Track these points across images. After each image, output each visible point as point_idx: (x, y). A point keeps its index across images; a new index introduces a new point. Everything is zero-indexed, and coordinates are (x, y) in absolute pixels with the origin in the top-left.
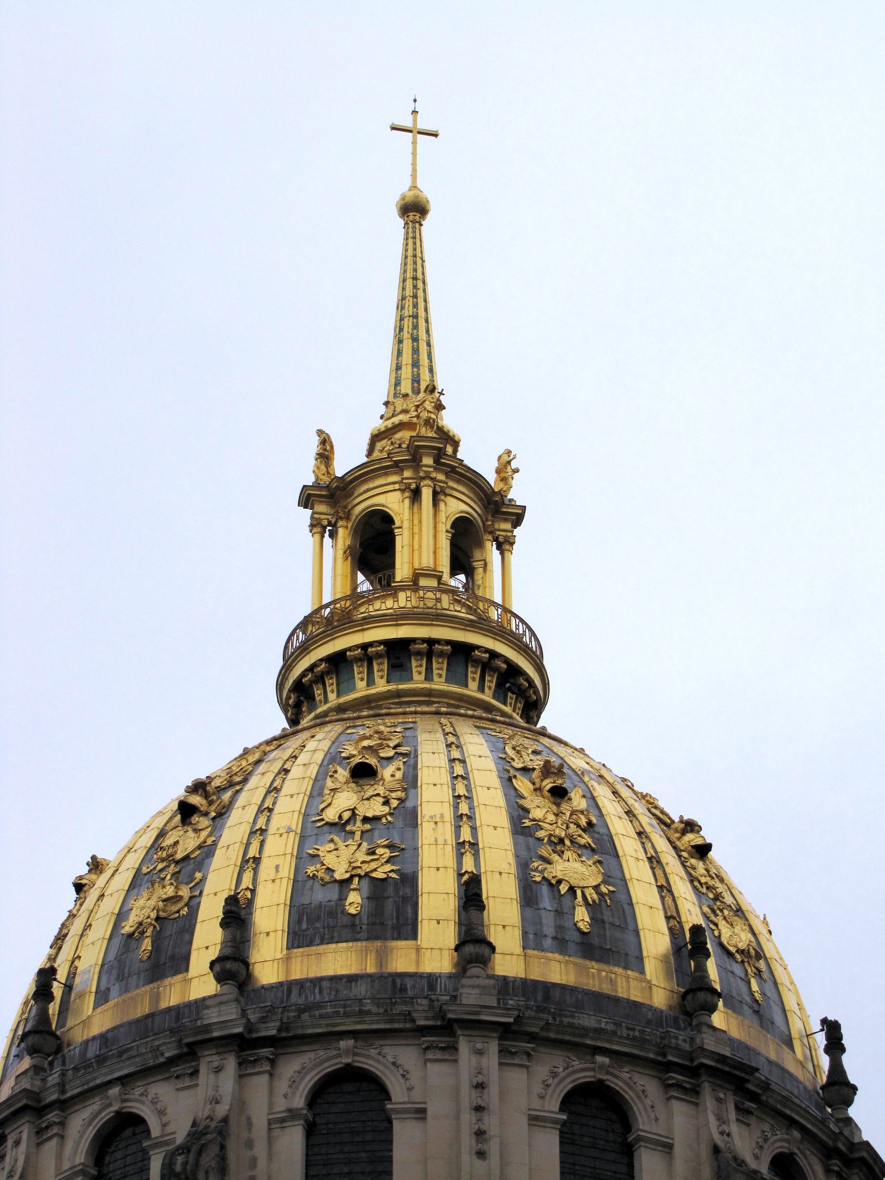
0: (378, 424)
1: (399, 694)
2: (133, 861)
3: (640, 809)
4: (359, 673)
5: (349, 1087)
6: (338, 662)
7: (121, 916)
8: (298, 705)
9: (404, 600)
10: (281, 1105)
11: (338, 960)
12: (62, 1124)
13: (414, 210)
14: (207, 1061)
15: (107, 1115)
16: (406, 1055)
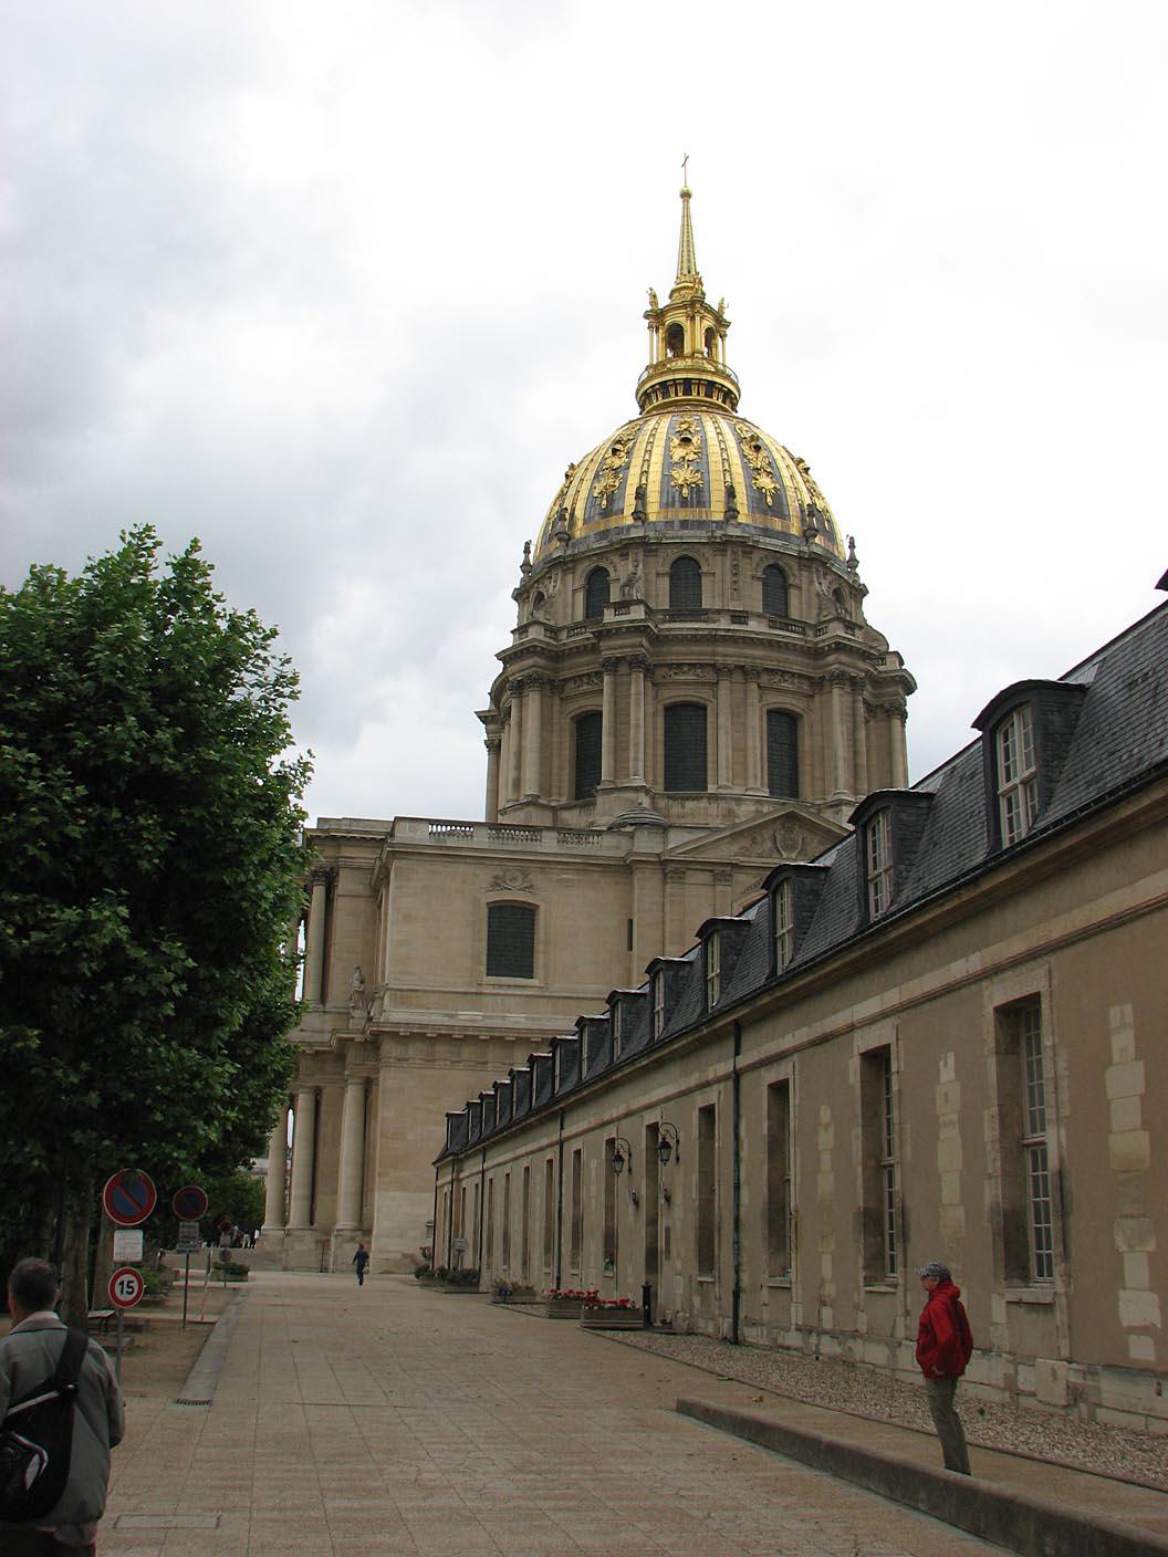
0: (673, 286)
2: (594, 467)
5: (686, 562)
7: (592, 488)
8: (644, 401)
10: (661, 570)
12: (574, 569)
13: (686, 195)
15: (589, 569)
16: (707, 552)
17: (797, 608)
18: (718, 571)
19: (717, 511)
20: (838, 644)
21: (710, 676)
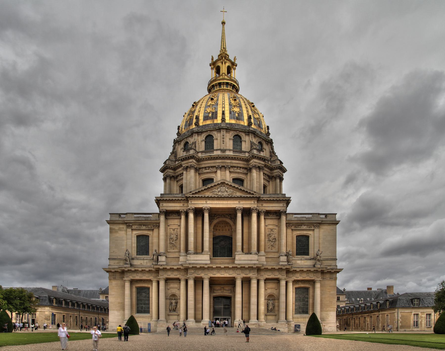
1: (220, 90)
3: (246, 101)
4: (216, 87)
6: (213, 86)
9: (221, 77)
11: (209, 122)
14: (194, 135)
16: (215, 133)
17: (245, 146)
18: (219, 138)
19: (219, 120)
20: (253, 156)
21: (214, 170)
